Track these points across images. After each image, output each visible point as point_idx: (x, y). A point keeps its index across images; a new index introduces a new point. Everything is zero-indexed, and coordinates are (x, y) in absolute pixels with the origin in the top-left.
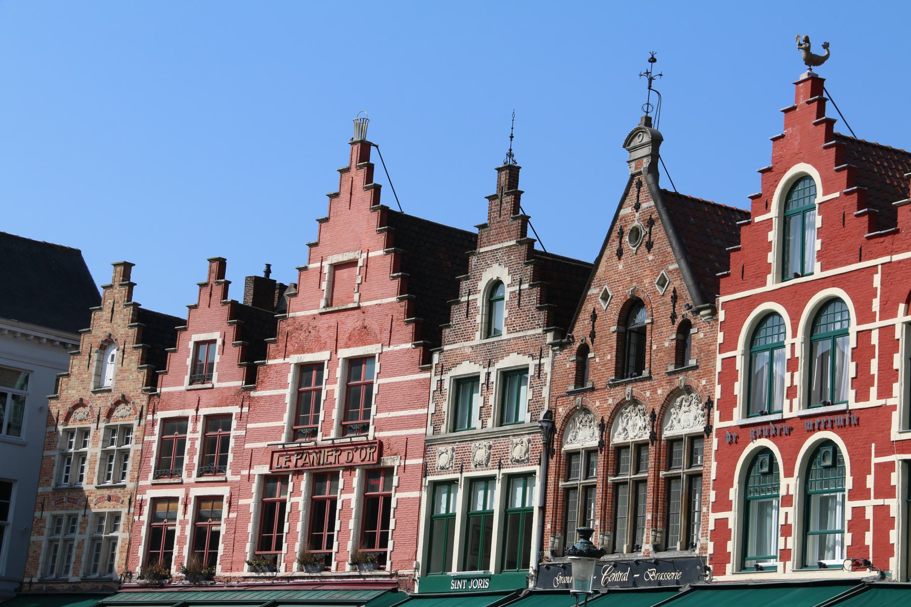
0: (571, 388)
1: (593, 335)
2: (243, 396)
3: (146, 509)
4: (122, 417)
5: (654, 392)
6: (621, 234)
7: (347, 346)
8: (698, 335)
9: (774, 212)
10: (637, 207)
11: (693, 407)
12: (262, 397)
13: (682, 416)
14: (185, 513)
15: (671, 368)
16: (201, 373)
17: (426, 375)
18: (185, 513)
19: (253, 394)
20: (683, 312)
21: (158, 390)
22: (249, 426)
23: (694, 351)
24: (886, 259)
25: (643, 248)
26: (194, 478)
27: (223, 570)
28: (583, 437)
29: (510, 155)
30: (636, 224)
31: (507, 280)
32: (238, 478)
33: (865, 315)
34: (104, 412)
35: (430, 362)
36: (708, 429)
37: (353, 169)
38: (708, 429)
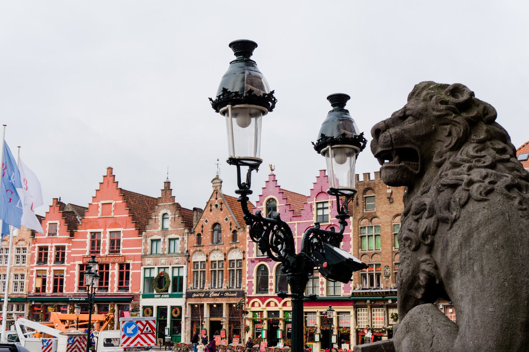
0: (195, 245)
1: (202, 231)
2: (68, 240)
4: (22, 244)
5: (225, 248)
6: (211, 206)
7: (109, 228)
8: (239, 234)
10: (216, 199)
11: (237, 252)
12: (77, 241)
13: (234, 254)
14: (50, 274)
15: (231, 242)
17: (141, 238)
18: (50, 274)
19: (73, 240)
20: (234, 228)
21: (36, 237)
22: (72, 249)
23: (238, 238)
24: (299, 222)
25: (219, 210)
26: (52, 264)
27: (66, 291)
28: (199, 258)
30: (216, 203)
31: (169, 213)
32: (69, 265)
34: (14, 243)
35: (142, 234)
36: (244, 259)
37: (108, 176)
38: (244, 259)
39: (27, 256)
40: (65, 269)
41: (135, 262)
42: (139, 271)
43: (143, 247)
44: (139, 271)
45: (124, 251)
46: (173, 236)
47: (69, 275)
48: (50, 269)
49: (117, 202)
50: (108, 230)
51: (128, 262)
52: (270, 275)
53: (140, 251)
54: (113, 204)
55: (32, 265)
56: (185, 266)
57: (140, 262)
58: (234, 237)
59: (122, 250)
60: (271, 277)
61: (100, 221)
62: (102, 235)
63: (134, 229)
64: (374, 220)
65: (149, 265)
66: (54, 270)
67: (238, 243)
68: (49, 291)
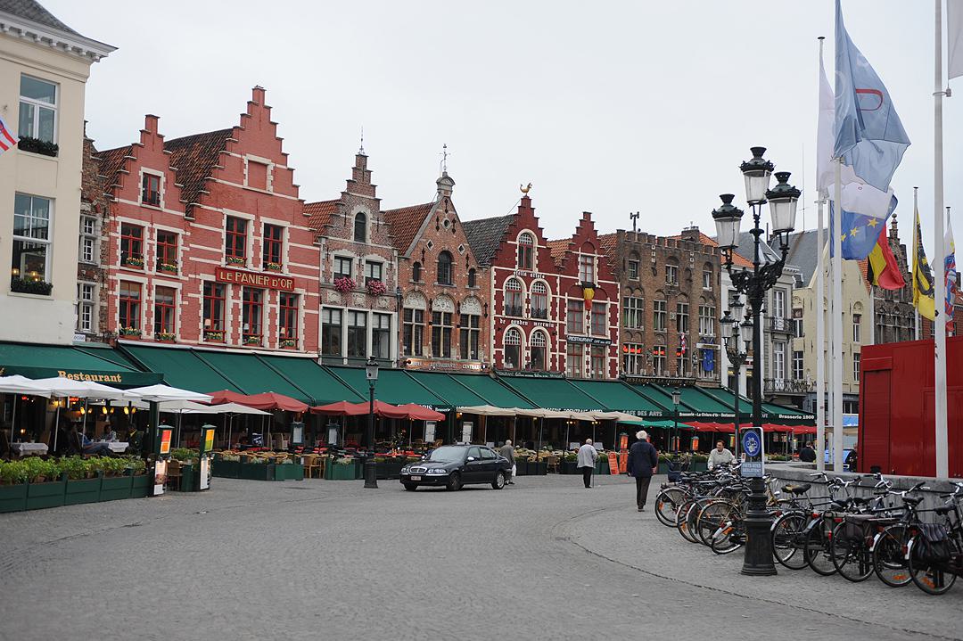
1: (423, 260)
2: (184, 223)
3: (118, 287)
5: (458, 294)
6: (438, 220)
8: (479, 276)
9: (517, 243)
10: (446, 211)
16: (151, 198)
17: (318, 249)
19: (192, 224)
22: (191, 245)
23: (478, 283)
26: (154, 271)
27: (182, 338)
29: (362, 149)
30: (447, 219)
32: (187, 279)
33: (554, 292)
38: (486, 315)
39: (99, 242)
40: (178, 286)
41: (310, 294)
42: (316, 312)
43: (323, 268)
44: (316, 312)
45: (292, 269)
46: (374, 257)
47: (187, 303)
48: (150, 283)
49: (277, 165)
50: (264, 220)
51: (298, 290)
52: (524, 344)
53: (316, 273)
54: (270, 168)
55: (111, 267)
56: (395, 315)
57: (317, 295)
58: (472, 281)
59: (289, 267)
60: (527, 348)
61: (248, 197)
62: (251, 228)
63: (306, 229)
64: (637, 292)
65: (335, 303)
66: (157, 286)
67: (478, 290)
68: (149, 334)
